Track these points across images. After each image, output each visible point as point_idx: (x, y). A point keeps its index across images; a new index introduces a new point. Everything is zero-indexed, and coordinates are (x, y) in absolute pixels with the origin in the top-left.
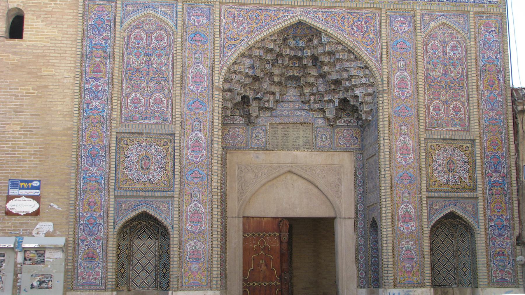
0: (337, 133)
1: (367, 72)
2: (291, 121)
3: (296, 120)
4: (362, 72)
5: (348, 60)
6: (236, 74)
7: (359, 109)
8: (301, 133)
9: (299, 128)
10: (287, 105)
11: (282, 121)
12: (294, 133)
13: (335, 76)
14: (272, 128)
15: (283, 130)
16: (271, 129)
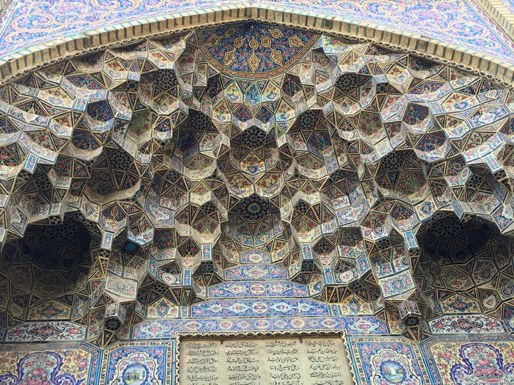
0: (440, 356)
1: (491, 94)
2: (263, 329)
3: (280, 327)
4: (472, 101)
5: (416, 86)
6: (40, 112)
7: (499, 223)
8: (304, 364)
9: (295, 351)
10: (242, 289)
11: (227, 330)
12: (276, 364)
13: (382, 146)
14: (190, 354)
15: (234, 357)
16: (189, 357)
